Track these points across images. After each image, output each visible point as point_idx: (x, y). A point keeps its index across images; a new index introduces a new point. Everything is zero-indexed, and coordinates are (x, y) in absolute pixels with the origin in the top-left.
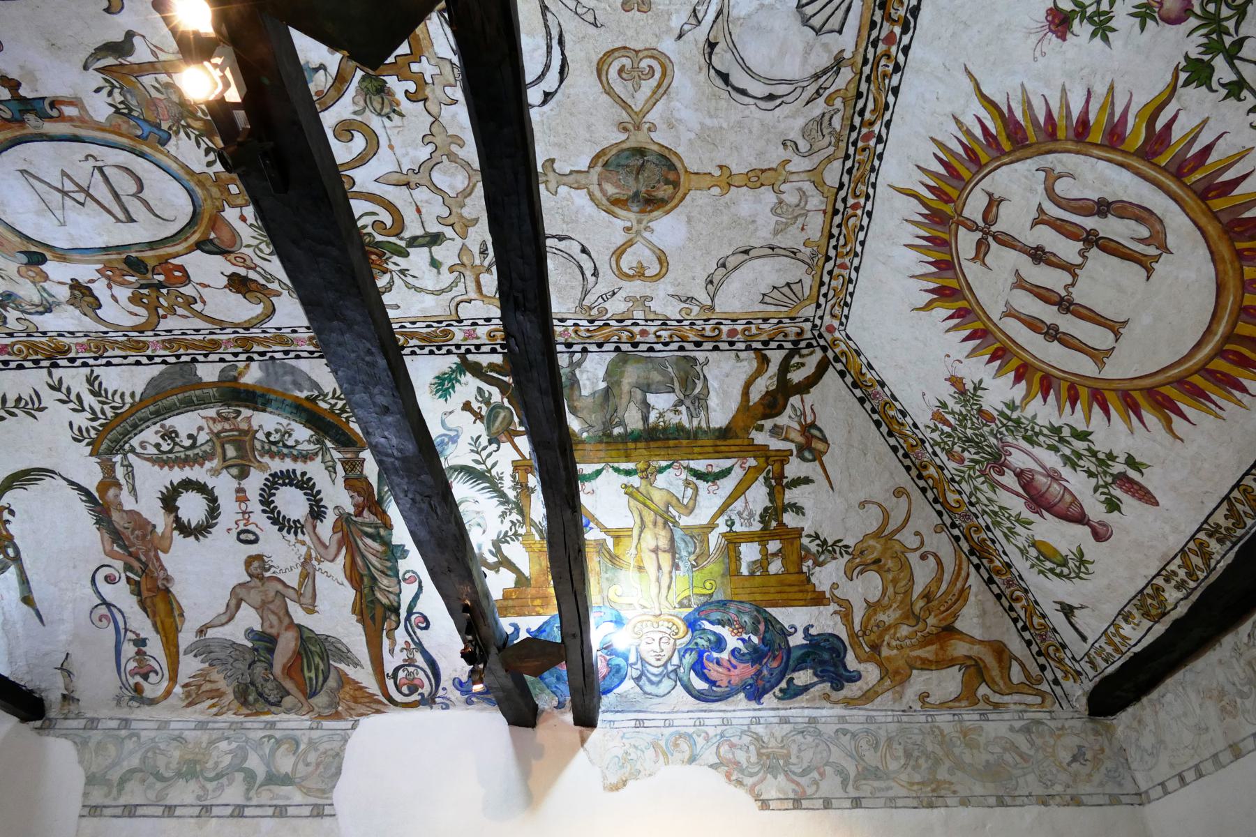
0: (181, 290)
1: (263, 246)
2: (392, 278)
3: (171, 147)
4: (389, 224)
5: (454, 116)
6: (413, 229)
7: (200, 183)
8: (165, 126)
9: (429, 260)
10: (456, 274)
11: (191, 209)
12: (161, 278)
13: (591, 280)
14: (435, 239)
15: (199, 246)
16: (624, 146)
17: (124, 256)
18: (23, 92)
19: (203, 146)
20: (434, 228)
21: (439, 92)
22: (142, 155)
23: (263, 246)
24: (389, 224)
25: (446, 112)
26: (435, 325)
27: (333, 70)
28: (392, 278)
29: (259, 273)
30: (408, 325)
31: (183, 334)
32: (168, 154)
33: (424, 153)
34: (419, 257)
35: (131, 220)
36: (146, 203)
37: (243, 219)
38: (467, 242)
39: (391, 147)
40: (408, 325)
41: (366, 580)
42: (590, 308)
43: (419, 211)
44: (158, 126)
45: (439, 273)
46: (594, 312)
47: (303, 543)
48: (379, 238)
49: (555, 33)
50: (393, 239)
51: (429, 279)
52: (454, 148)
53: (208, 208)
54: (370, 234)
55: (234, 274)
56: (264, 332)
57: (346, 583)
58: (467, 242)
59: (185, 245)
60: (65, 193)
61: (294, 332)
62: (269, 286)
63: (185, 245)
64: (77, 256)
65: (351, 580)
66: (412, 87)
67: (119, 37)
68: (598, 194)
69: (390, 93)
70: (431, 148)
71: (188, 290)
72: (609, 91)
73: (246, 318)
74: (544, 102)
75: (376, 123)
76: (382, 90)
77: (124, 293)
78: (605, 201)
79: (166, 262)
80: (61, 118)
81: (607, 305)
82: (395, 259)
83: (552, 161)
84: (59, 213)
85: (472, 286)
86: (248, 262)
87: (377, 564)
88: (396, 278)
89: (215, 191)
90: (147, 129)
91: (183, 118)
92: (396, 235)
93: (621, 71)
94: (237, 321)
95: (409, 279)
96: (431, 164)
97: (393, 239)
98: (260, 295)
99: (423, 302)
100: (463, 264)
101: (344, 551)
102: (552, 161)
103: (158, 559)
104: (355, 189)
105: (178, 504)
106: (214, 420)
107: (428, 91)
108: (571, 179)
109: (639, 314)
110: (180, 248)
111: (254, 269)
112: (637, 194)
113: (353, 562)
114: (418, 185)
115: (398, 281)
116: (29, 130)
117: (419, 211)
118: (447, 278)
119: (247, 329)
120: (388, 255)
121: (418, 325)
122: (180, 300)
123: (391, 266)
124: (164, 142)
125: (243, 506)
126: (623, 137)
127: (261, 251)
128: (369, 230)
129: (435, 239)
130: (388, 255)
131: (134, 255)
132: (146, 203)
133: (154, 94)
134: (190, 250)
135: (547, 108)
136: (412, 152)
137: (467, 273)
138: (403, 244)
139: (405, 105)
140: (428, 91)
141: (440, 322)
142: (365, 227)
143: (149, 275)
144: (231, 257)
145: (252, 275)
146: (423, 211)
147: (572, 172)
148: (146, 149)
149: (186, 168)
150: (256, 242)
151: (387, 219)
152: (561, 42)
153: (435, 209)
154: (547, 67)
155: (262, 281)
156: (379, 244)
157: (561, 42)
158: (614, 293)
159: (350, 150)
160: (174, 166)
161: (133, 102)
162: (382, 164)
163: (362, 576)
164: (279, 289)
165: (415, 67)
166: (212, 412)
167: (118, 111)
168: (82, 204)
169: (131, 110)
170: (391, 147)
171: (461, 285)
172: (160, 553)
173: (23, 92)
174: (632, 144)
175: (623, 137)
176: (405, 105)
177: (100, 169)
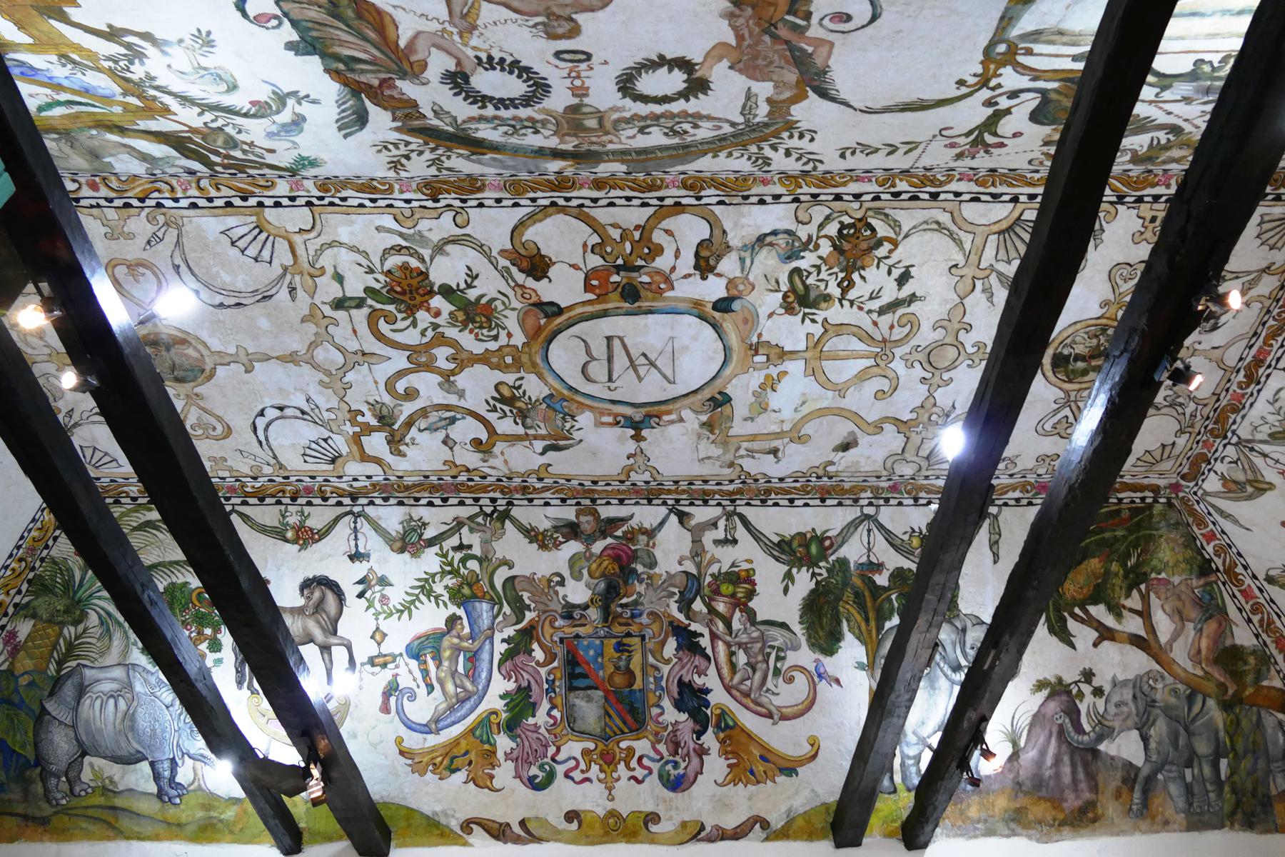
0: (601, 262)
1: (500, 307)
2: (382, 264)
3: (546, 392)
4: (382, 321)
5: (328, 400)
6: (360, 315)
7: (534, 365)
8: (544, 406)
9: (345, 283)
10: (317, 266)
11: (551, 346)
12: (615, 278)
13: (178, 261)
14: (339, 304)
15: (560, 311)
16: (192, 384)
17: (636, 304)
18: (633, 432)
19: (521, 391)
20: (341, 315)
21: (340, 415)
22: (571, 388)
23: (500, 307)
24: (382, 321)
25: (334, 402)
26: (337, 201)
27: (414, 429)
28: (382, 264)
29: (514, 280)
30: (367, 203)
31: (629, 199)
32: (550, 387)
33: (350, 377)
34: (355, 288)
35: (609, 339)
36: (588, 352)
37: (509, 335)
38: (309, 300)
39: (376, 382)
40: (367, 203)
41: (350, 13)
42: (166, 224)
43: (355, 332)
44: (548, 406)
45: (335, 267)
46: (161, 219)
47: (474, 48)
48: (391, 308)
49: (265, 447)
50: (379, 306)
51: (345, 260)
52: (326, 379)
53: (536, 347)
54: (400, 311)
55: (538, 279)
56: (534, 200)
57: (389, 9)
58: (309, 300)
59: (572, 313)
60: (652, 364)
61: (498, 201)
62: (507, 263)
63: (572, 313)
64: (682, 306)
65: (379, 12)
66: (360, 418)
67: (551, 454)
68: (201, 347)
69: (374, 415)
70: (345, 380)
71: (595, 261)
72: (219, 419)
73: (549, 220)
74: (263, 410)
75: (387, 399)
76: (381, 418)
77: (663, 263)
78: (193, 342)
79: (599, 296)
80: (616, 416)
81: (150, 229)
82: (377, 286)
83: (247, 372)
84: (669, 349)
85: (300, 251)
86: (519, 292)
87: (338, 33)
88: (378, 265)
89: (525, 359)
90: (558, 407)
91: (528, 410)
92: (375, 310)
93: (214, 429)
94: (561, 216)
95: (365, 262)
96: (345, 368)
97: (379, 306)
98: (523, 252)
99: (351, 233)
100: (312, 276)
101: (402, 43)
102: (247, 372)
103: (740, 38)
104: (408, 353)
105: (685, 85)
106: (611, 142)
107: (348, 416)
108: (228, 359)
109: (111, 214)
110: (579, 310)
111: (517, 285)
112: (168, 349)
113: (381, 31)
114: (355, 353)
115: (376, 260)
116: (644, 411)
117: (355, 332)
118: (326, 261)
119: (554, 204)
120: (384, 291)
121: (356, 202)
122: (609, 249)
123: (382, 278)
124: (551, 396)
125: (578, 83)
126: (197, 390)
127: (504, 303)
128: (400, 316)
129: (339, 304)
130: (384, 291)
131: (627, 305)
132: (588, 352)
133: (542, 425)
134: (570, 308)
135: (261, 407)
136: (360, 377)
137: (306, 266)
138: (370, 302)
139: (365, 408)
140: (348, 416)
141: (332, 204)
142: (403, 319)
143: (625, 281)
144: (534, 299)
145: (520, 277)
146: (351, 331)
147: (229, 364)
148: (566, 392)
149: (540, 376)
150: (506, 313)
151: (383, 326)
152: (260, 443)
153: (341, 334)
154: (266, 429)
155: (514, 270)
156: (392, 301)
157: (260, 443)
158: (149, 242)
159: (408, 382)
160: (550, 379)
161: (559, 423)
162: (384, 371)
163: (359, 16)
164: (499, 258)
165: (358, 429)
166: (610, 147)
167: (573, 417)
168: (644, 355)
169: (563, 418)
170: (376, 382)
171: (311, 252)
172: (733, 42)
173: (633, 432)
174: (189, 386)
175: (197, 390)
176: (365, 408)
177: (610, 380)
